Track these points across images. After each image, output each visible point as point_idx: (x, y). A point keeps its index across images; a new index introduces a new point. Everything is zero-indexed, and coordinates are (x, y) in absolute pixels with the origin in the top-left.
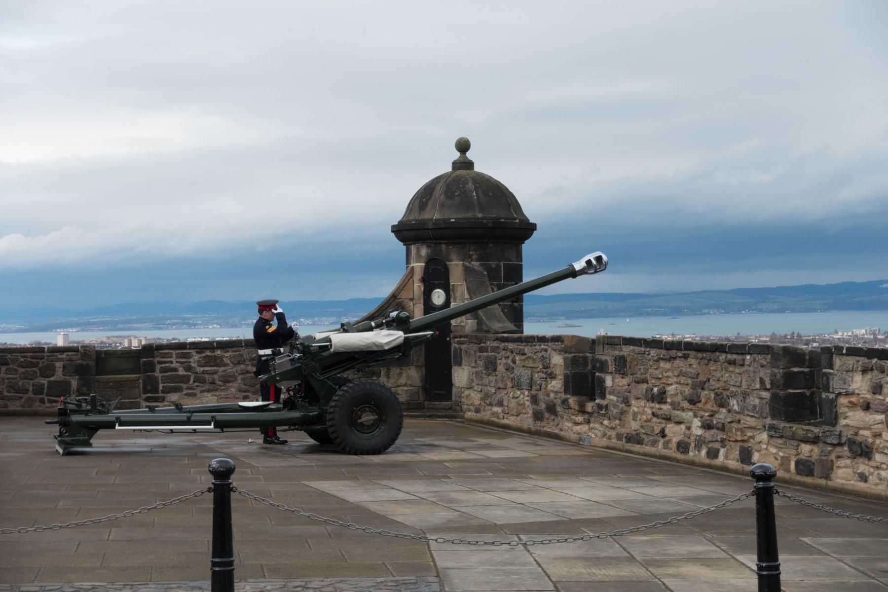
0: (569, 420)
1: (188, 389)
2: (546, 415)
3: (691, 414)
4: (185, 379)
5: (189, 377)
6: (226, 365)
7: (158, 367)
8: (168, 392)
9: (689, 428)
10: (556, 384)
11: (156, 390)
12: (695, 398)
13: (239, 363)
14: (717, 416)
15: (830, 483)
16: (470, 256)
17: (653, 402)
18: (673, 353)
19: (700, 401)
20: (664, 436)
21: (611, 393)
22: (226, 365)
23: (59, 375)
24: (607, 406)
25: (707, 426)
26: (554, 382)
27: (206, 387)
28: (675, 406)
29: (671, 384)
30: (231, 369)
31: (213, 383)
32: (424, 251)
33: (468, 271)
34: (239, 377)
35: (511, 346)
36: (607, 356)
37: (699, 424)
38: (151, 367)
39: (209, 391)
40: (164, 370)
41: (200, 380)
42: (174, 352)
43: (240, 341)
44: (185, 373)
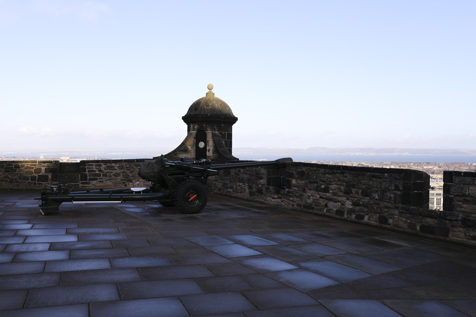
1: (100, 179)
2: (257, 194)
3: (345, 198)
4: (99, 175)
7: (87, 170)
10: (263, 181)
11: (86, 179)
13: (122, 169)
15: (447, 239)
16: (215, 129)
21: (294, 186)
25: (355, 204)
26: (261, 181)
28: (334, 194)
30: (118, 171)
32: (196, 127)
33: (214, 135)
39: (108, 180)
41: (105, 175)
42: (94, 164)
43: (122, 160)
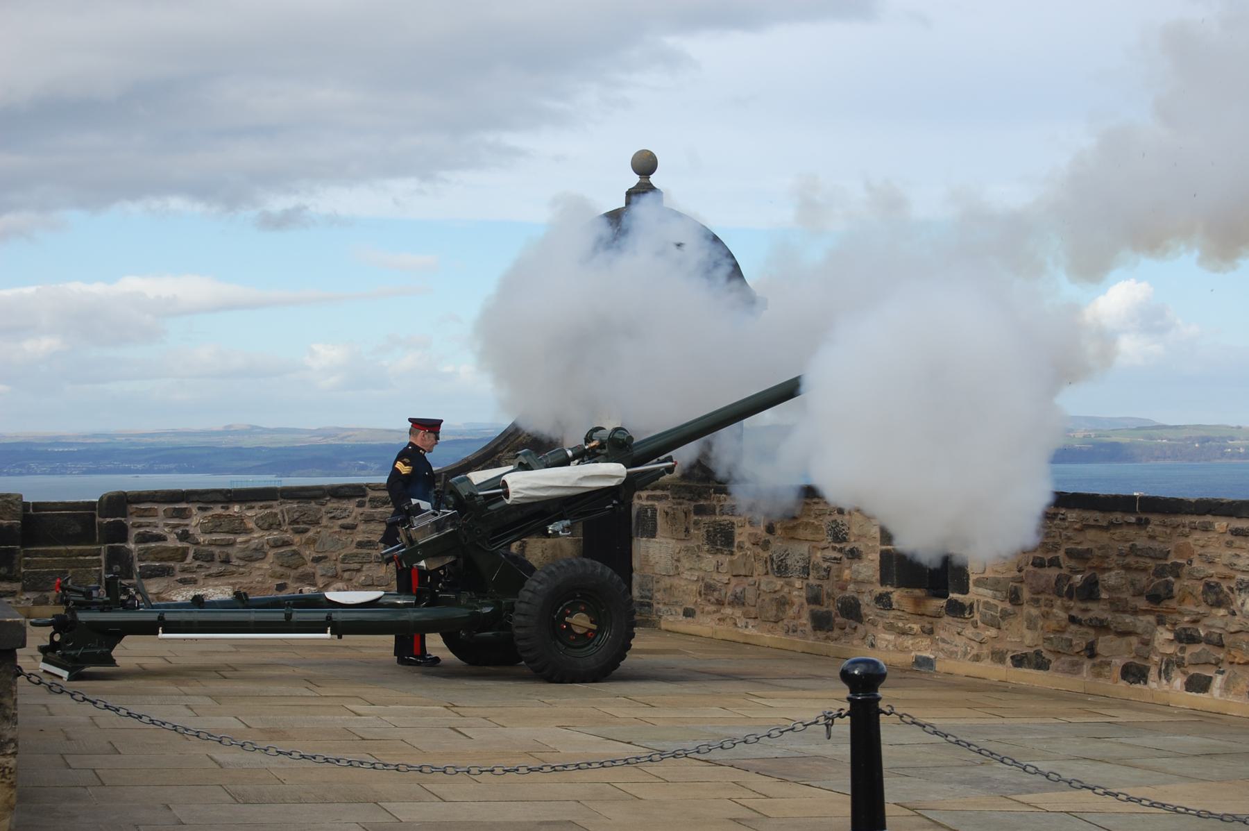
0: (890, 628)
1: (184, 570)
4: (181, 555)
5: (184, 552)
6: (248, 531)
7: (134, 533)
8: (150, 577)
9: (1146, 643)
12: (1162, 591)
13: (270, 528)
14: (1207, 621)
17: (1071, 598)
18: (1117, 516)
19: (1172, 597)
21: (980, 583)
22: (251, 531)
24: (972, 605)
27: (214, 569)
28: (1117, 606)
29: (1110, 569)
30: (258, 537)
31: (226, 561)
34: (271, 553)
37: (1171, 636)
38: (119, 532)
39: (219, 575)
40: (143, 538)
44: (179, 545)
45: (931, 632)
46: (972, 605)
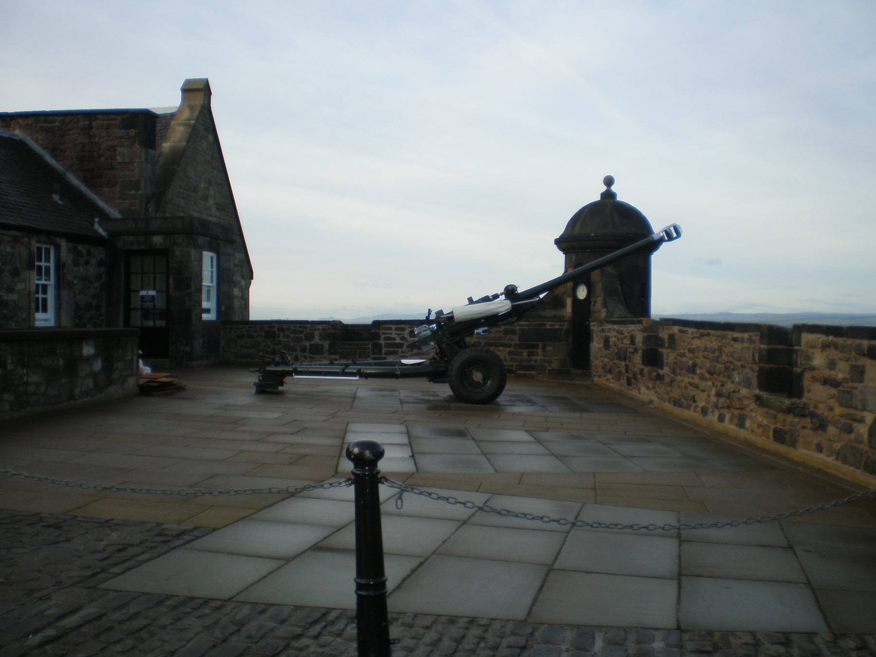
1: (403, 352)
4: (400, 346)
7: (383, 336)
9: (709, 396)
10: (638, 358)
11: (380, 352)
20: (695, 401)
23: (316, 340)
28: (702, 378)
35: (616, 327)
36: (664, 334)
38: (377, 336)
42: (394, 327)
45: (654, 388)
46: (663, 376)
